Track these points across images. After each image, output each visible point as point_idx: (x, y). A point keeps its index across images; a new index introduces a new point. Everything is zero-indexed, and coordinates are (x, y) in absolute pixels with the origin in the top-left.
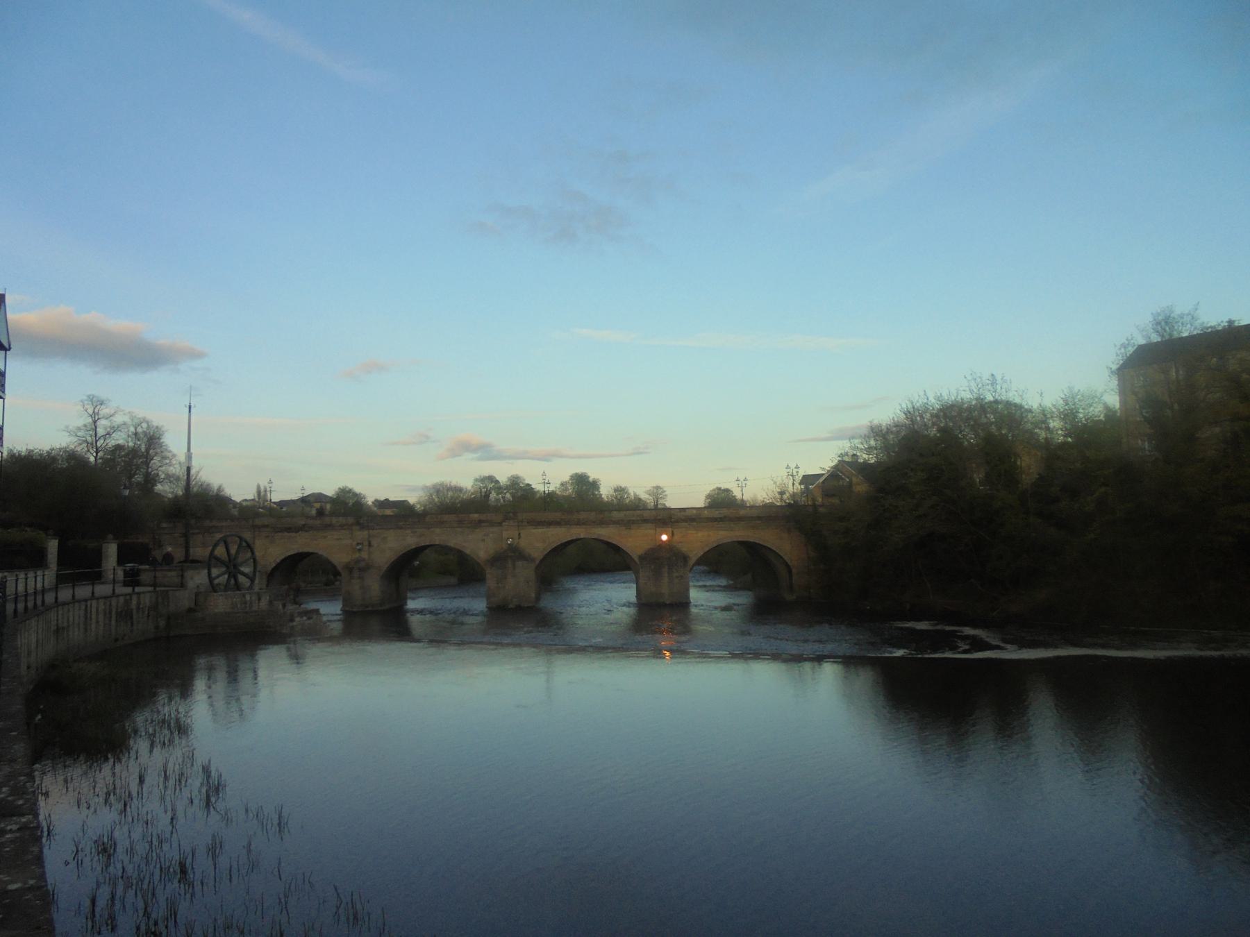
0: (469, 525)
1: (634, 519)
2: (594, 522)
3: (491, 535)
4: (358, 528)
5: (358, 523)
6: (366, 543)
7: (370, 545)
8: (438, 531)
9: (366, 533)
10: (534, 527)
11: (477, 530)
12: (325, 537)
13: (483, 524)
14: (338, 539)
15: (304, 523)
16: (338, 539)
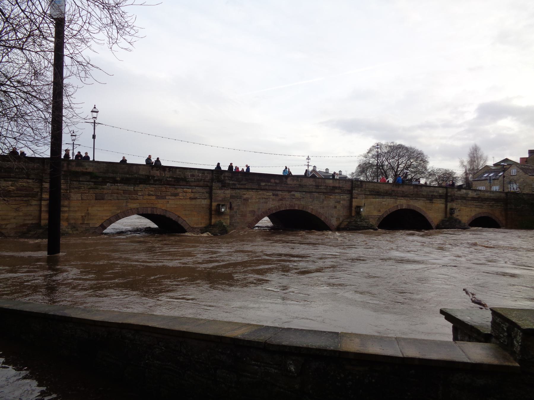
0: (325, 191)
1: (435, 194)
2: (412, 195)
3: (341, 202)
4: (220, 185)
5: (219, 181)
6: (228, 206)
7: (231, 208)
8: (298, 195)
9: (228, 192)
10: (374, 197)
11: (331, 197)
12: (176, 195)
13: (337, 191)
14: (191, 199)
15: (148, 174)
16: (191, 199)
